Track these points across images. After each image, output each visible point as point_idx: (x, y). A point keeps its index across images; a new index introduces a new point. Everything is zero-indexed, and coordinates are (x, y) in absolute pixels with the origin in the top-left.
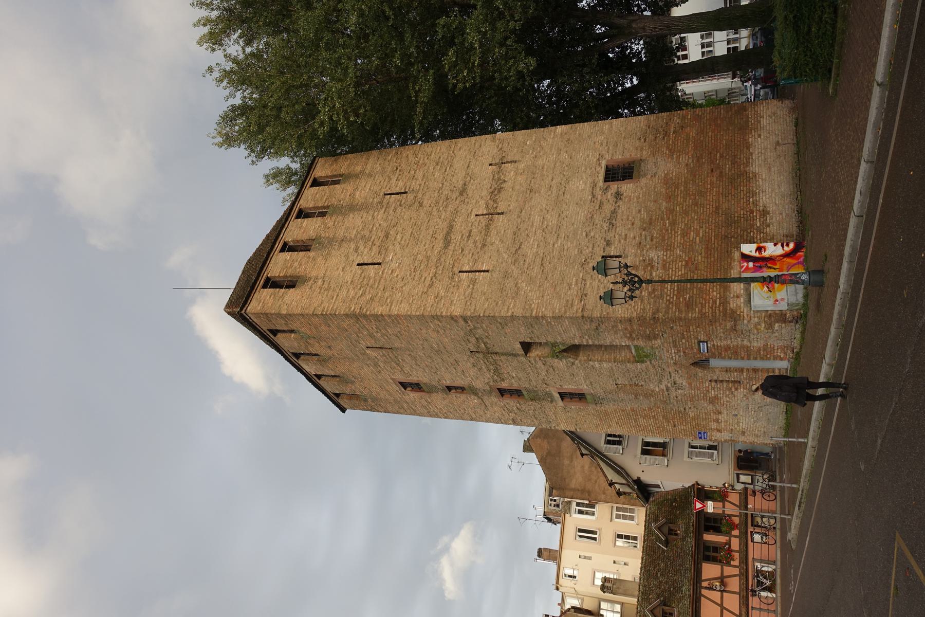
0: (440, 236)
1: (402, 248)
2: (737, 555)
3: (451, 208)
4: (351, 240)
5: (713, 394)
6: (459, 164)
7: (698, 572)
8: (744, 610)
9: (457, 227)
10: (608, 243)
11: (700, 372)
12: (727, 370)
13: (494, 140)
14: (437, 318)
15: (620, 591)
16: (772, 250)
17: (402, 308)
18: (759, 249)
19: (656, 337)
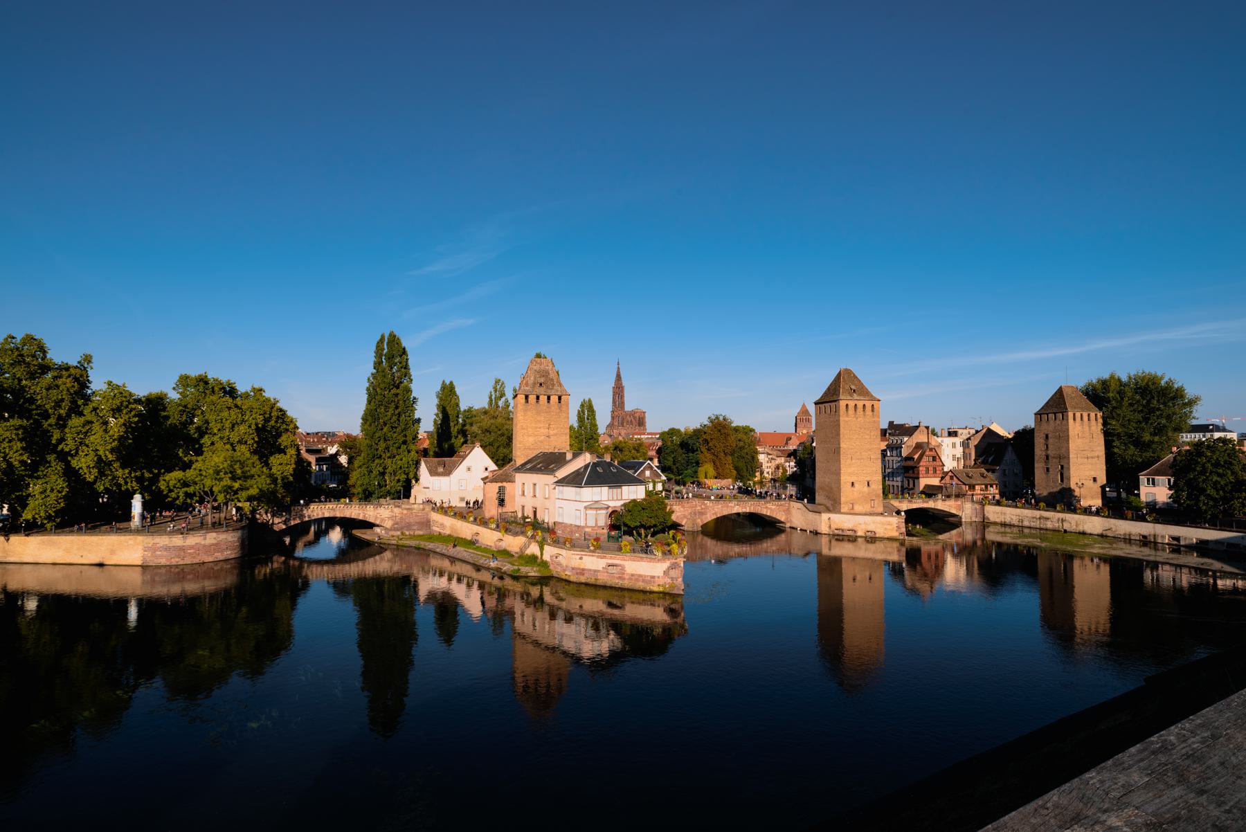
6: (1099, 448)
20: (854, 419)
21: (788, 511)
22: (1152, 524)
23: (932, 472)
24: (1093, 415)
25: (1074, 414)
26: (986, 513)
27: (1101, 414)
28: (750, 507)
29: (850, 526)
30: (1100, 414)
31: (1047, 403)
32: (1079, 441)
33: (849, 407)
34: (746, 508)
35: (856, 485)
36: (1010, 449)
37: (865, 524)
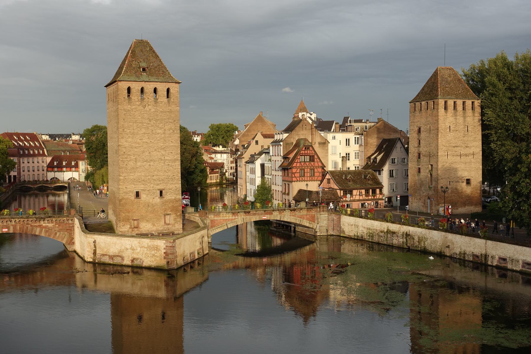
0: (456, 145)
1: (454, 136)
2: (368, 198)
3: (463, 145)
4: (456, 121)
5: (422, 199)
6: (474, 144)
7: (363, 189)
8: (356, 200)
9: (458, 148)
10: (452, 182)
11: (427, 197)
12: (427, 202)
13: (480, 151)
14: (438, 149)
15: (344, 163)
16: (450, 211)
17: (439, 141)
18: (450, 209)
19: (434, 191)
20: (141, 108)
21: (71, 230)
22: (483, 241)
23: (308, 174)
24: (469, 103)
25: (446, 102)
26: (341, 226)
27: (479, 101)
28: (14, 227)
29: (113, 250)
30: (477, 103)
31: (423, 89)
32: (451, 136)
33: (133, 91)
34: (8, 228)
35: (143, 196)
36: (399, 145)
37: (133, 250)
